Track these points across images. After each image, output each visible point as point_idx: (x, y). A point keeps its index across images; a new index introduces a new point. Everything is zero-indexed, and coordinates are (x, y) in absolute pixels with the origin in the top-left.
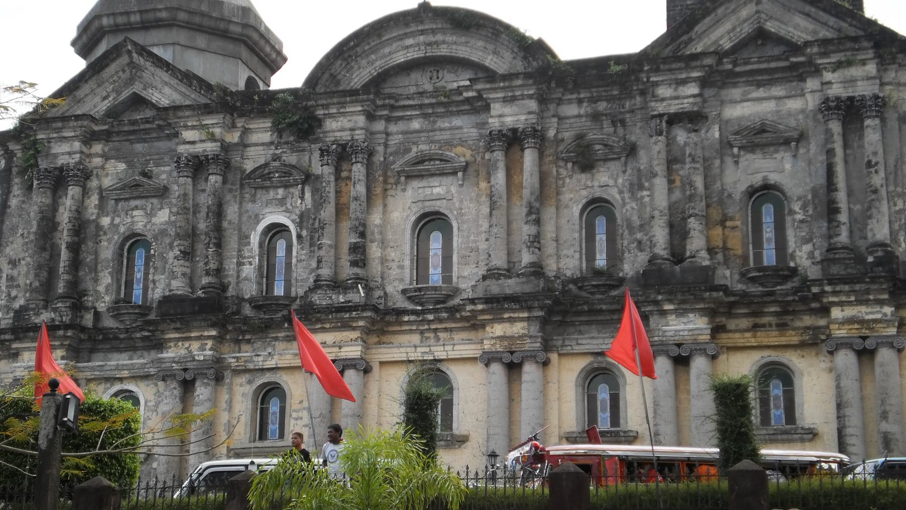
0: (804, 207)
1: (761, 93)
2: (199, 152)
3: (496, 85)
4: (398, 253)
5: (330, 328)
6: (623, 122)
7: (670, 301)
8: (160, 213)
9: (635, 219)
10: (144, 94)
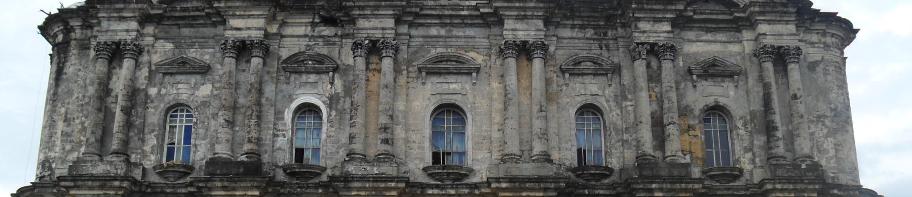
0: (745, 125)
1: (709, 37)
2: (244, 37)
3: (513, 5)
4: (419, 136)
6: (607, 46)
7: (661, 190)
8: (203, 88)
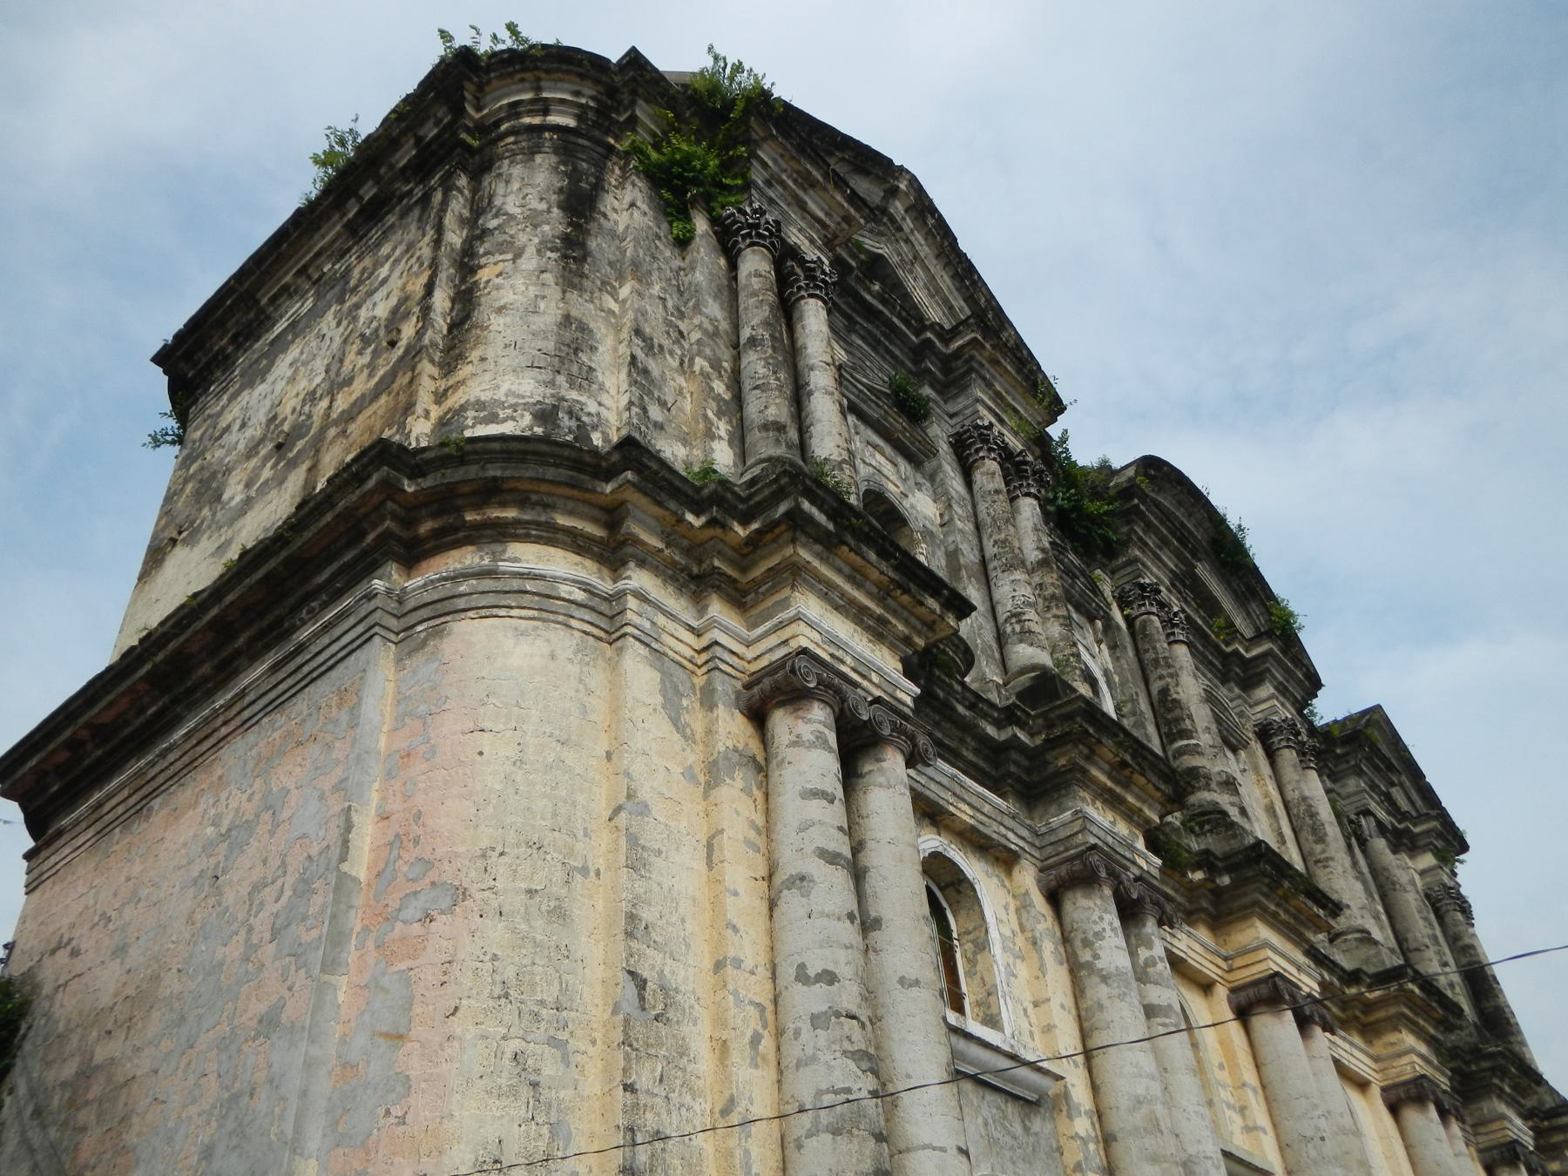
5: (1282, 922)
10: (900, 273)
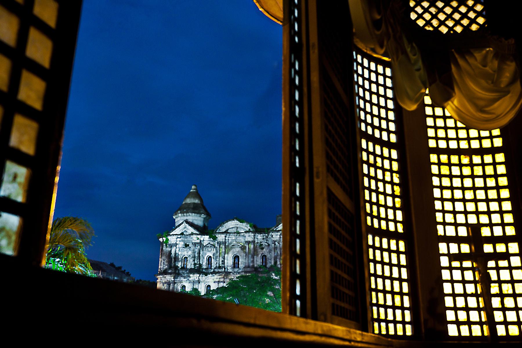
9: (270, 259)
